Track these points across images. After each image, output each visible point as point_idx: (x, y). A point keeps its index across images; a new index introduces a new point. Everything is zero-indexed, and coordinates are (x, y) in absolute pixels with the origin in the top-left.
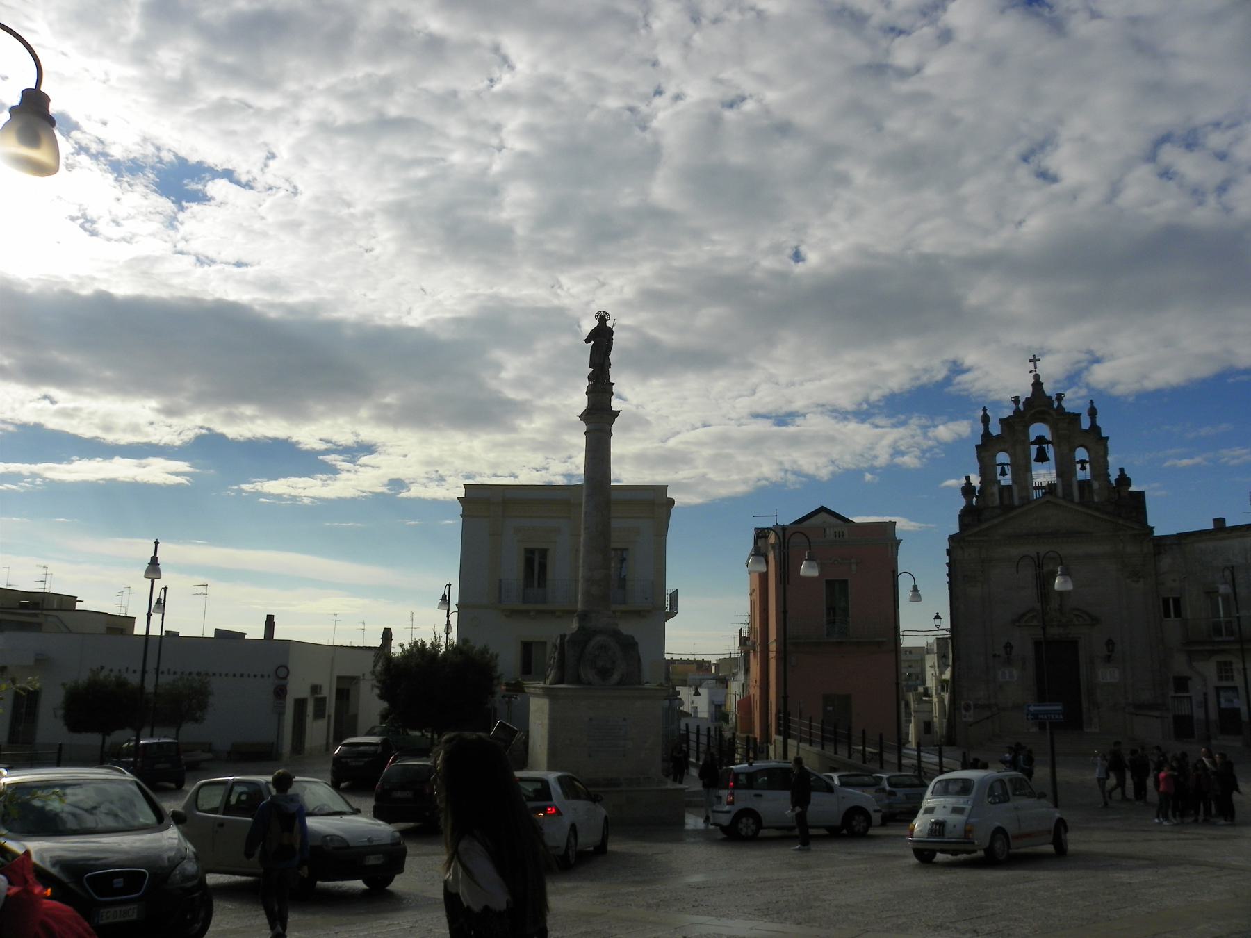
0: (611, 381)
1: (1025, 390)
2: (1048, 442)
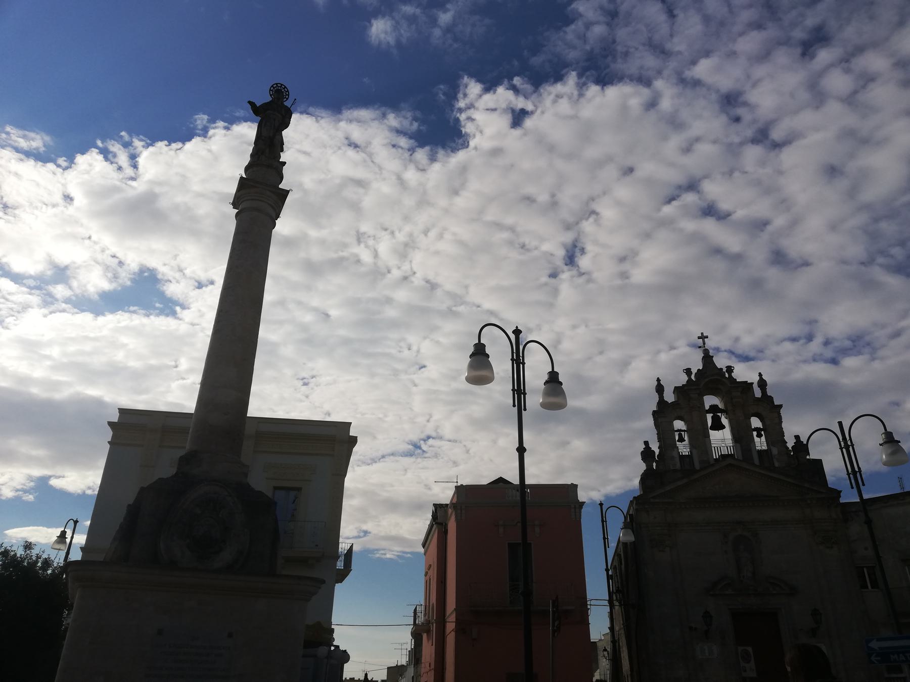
1: (697, 365)
2: (722, 411)
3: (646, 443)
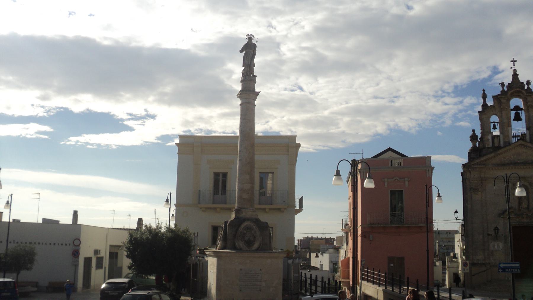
0: (255, 74)
2: (521, 109)
3: (473, 131)
